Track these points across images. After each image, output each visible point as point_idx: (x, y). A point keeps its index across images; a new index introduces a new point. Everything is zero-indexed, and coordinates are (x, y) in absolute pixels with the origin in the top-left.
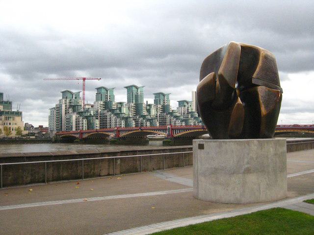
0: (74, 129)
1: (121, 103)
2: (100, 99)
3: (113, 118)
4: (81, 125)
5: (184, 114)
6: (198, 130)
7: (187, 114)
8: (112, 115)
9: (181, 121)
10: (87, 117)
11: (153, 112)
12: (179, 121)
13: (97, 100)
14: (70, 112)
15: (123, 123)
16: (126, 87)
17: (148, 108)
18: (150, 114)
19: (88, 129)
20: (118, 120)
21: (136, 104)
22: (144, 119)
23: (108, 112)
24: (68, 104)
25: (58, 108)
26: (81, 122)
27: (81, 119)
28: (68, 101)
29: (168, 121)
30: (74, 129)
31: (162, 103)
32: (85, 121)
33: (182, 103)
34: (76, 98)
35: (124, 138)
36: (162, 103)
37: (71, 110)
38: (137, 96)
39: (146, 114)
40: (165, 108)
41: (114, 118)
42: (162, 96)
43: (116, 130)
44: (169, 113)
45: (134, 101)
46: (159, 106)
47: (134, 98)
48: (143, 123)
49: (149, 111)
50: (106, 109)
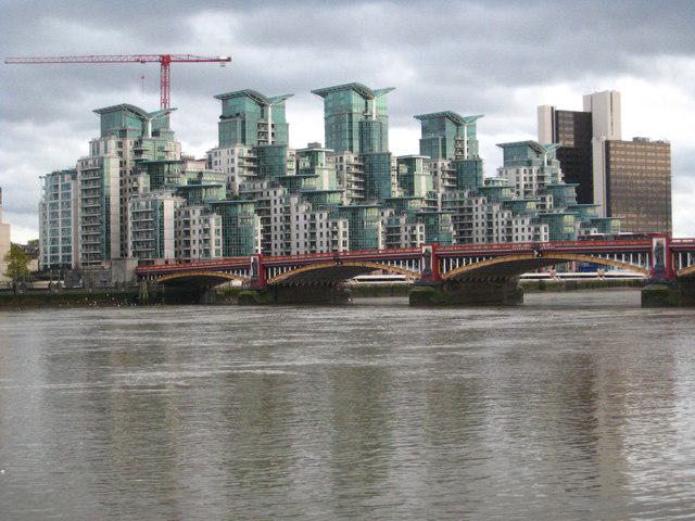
0: (169, 253)
1: (311, 153)
2: (239, 140)
3: (300, 210)
4: (195, 237)
5: (526, 193)
7: (540, 192)
8: (294, 200)
9: (533, 221)
10: (217, 207)
11: (423, 185)
12: (527, 221)
13: (226, 139)
15: (342, 226)
16: (323, 93)
17: (404, 170)
19: (227, 252)
20: (322, 218)
21: (363, 157)
22: (398, 213)
23: (272, 185)
24: (129, 156)
25: (91, 173)
26: (196, 227)
27: (196, 214)
28: (129, 145)
29: (480, 221)
30: (169, 253)
32: (215, 222)
33: (515, 153)
34: (155, 133)
35: (453, 283)
36: (451, 153)
37: (144, 181)
38: (366, 129)
40: (464, 172)
41: (303, 208)
42: (450, 127)
43: (427, 255)
44: (484, 191)
45: (356, 144)
46: (444, 164)
47: (356, 135)
48: (398, 229)
49: (407, 182)
50: (260, 178)
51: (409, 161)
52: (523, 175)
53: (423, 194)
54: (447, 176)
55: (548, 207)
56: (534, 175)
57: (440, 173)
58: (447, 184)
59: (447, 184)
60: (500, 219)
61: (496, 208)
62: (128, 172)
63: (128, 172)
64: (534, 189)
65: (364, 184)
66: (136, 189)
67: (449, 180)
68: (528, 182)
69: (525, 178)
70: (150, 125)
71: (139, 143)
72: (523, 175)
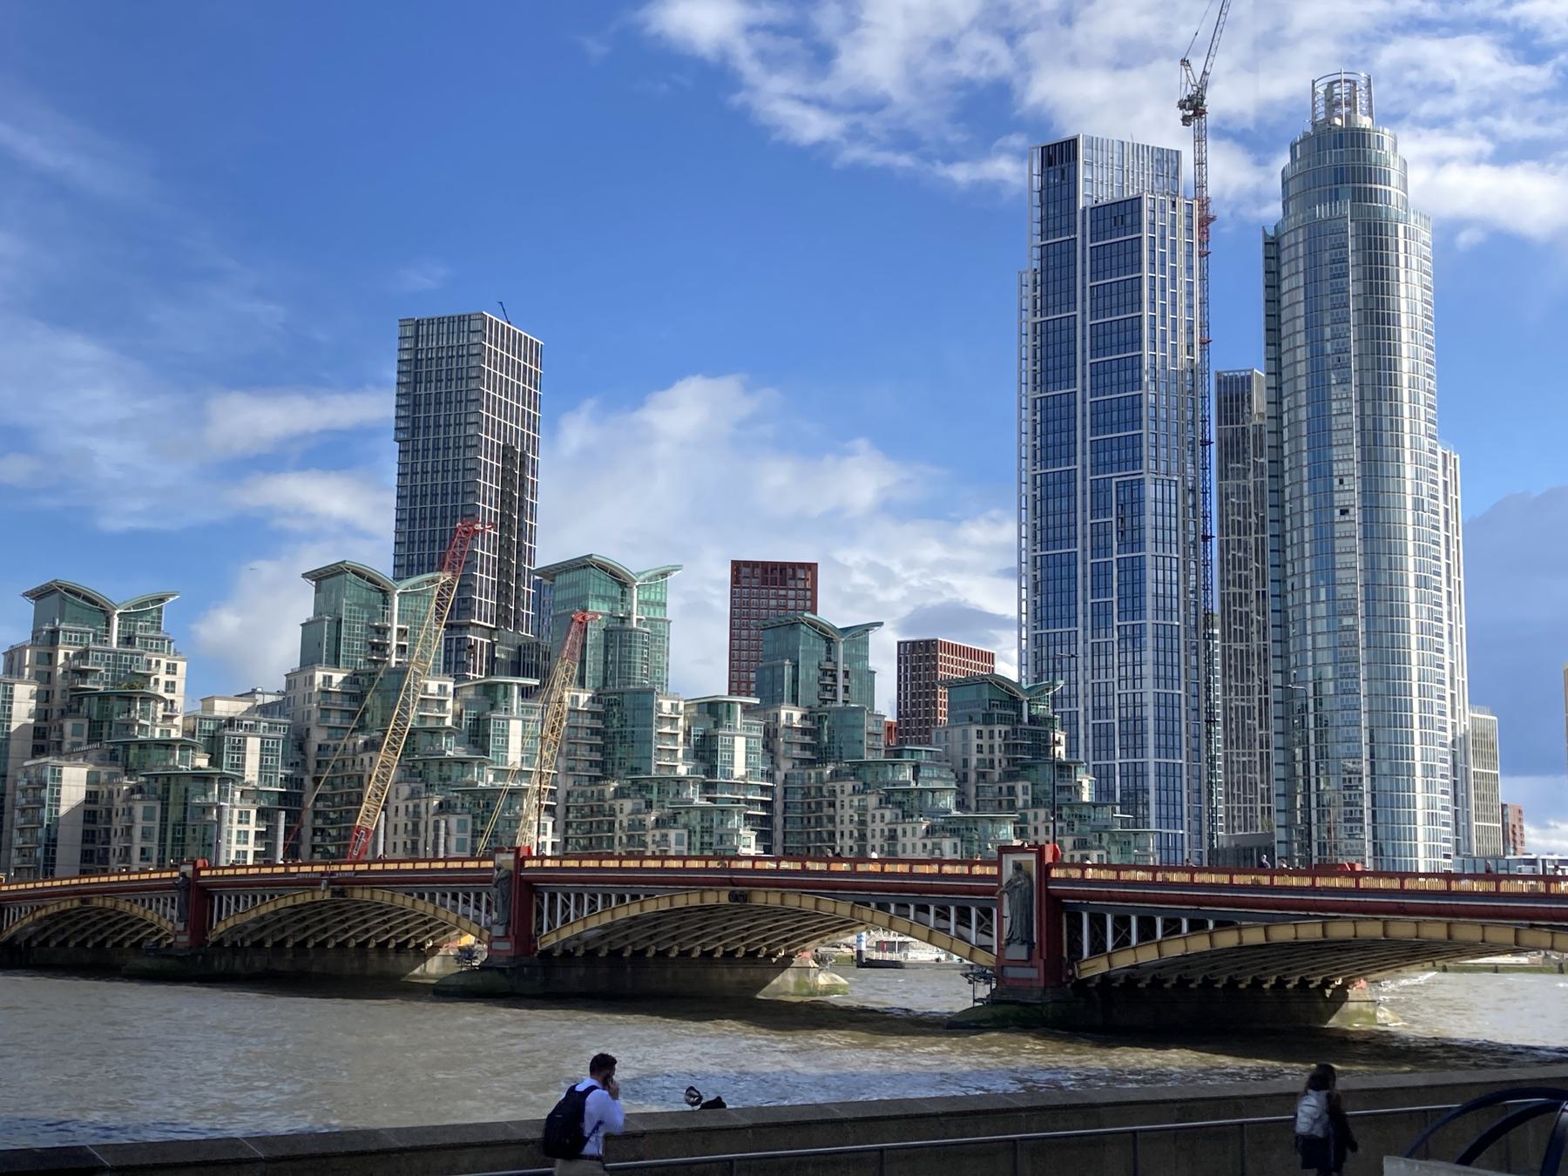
6: (694, 900)
7: (1010, 776)
14: (69, 739)
18: (711, 771)
24: (59, 684)
26: (118, 824)
31: (809, 693)
34: (128, 640)
39: (682, 770)
51: (712, 709)
52: (975, 742)
53: (739, 770)
54: (798, 737)
55: (1020, 803)
56: (998, 741)
57: (782, 732)
58: (796, 752)
59: (796, 752)
60: (878, 826)
61: (872, 801)
62: (56, 714)
63: (56, 714)
64: (997, 771)
65: (601, 749)
66: (59, 744)
67: (804, 747)
68: (986, 755)
69: (980, 749)
70: (116, 621)
71: (83, 655)
72: (975, 742)
